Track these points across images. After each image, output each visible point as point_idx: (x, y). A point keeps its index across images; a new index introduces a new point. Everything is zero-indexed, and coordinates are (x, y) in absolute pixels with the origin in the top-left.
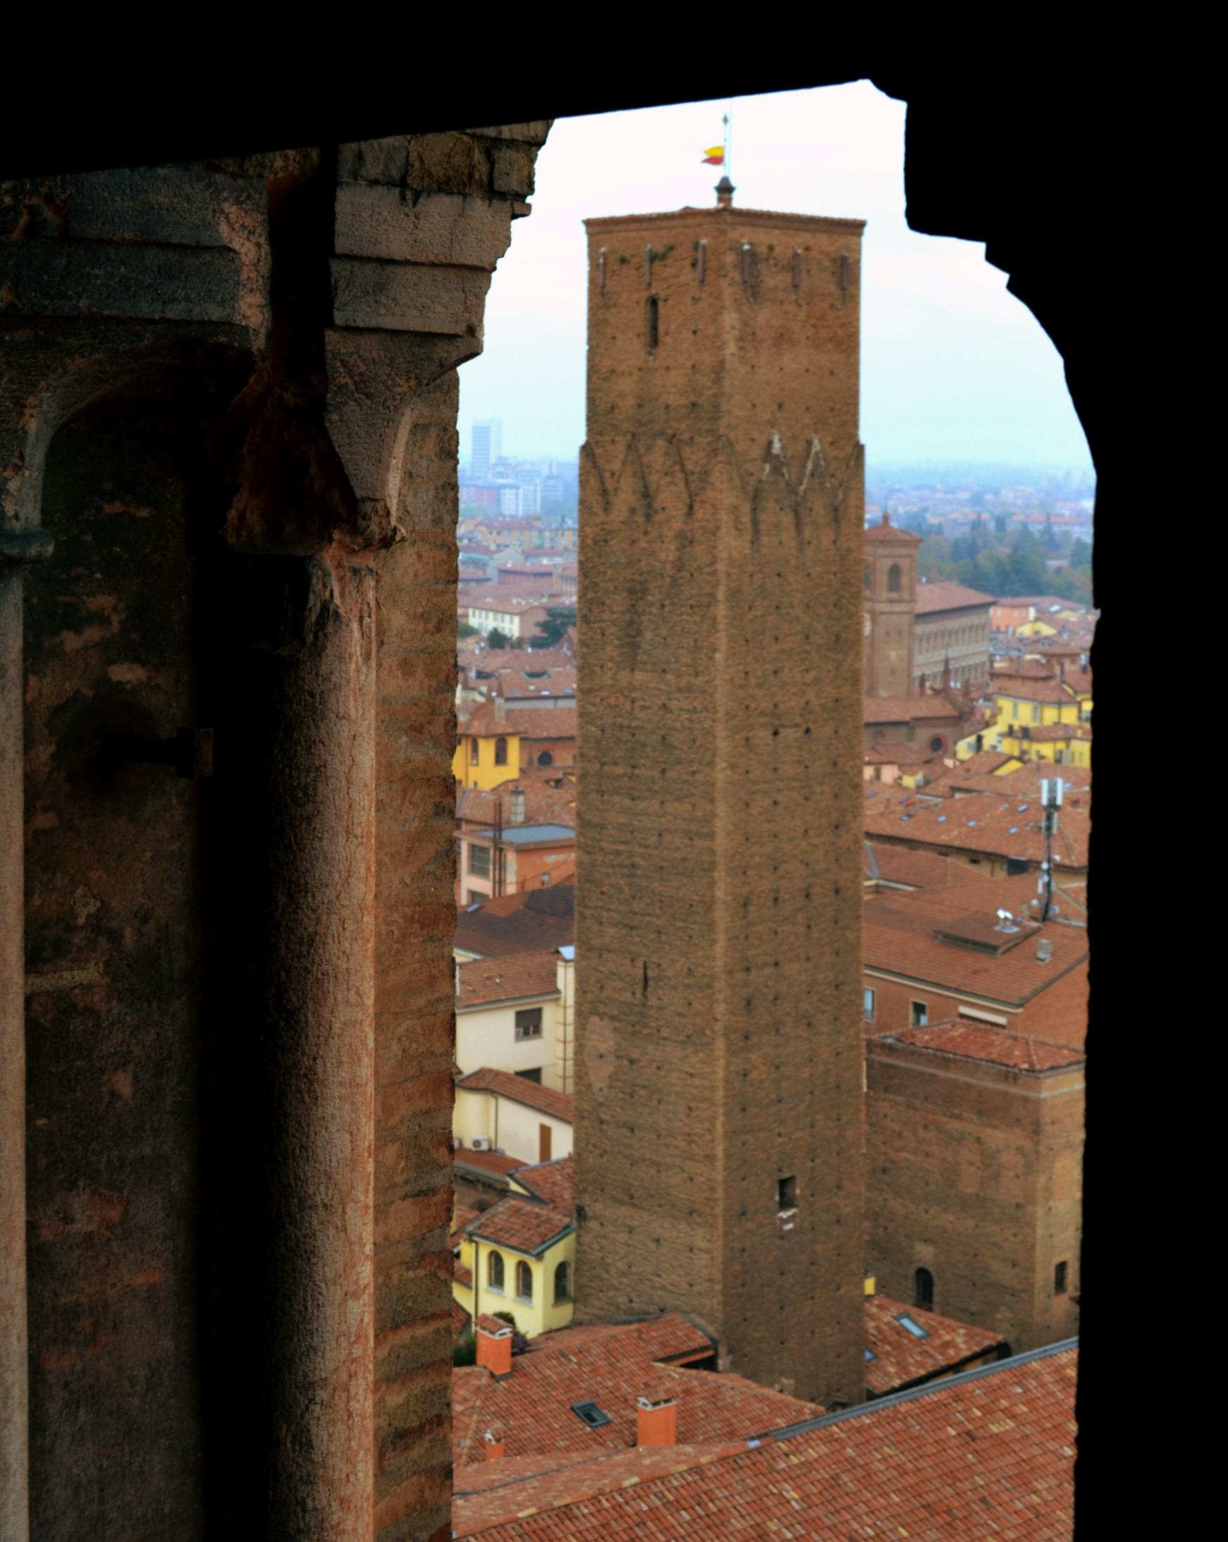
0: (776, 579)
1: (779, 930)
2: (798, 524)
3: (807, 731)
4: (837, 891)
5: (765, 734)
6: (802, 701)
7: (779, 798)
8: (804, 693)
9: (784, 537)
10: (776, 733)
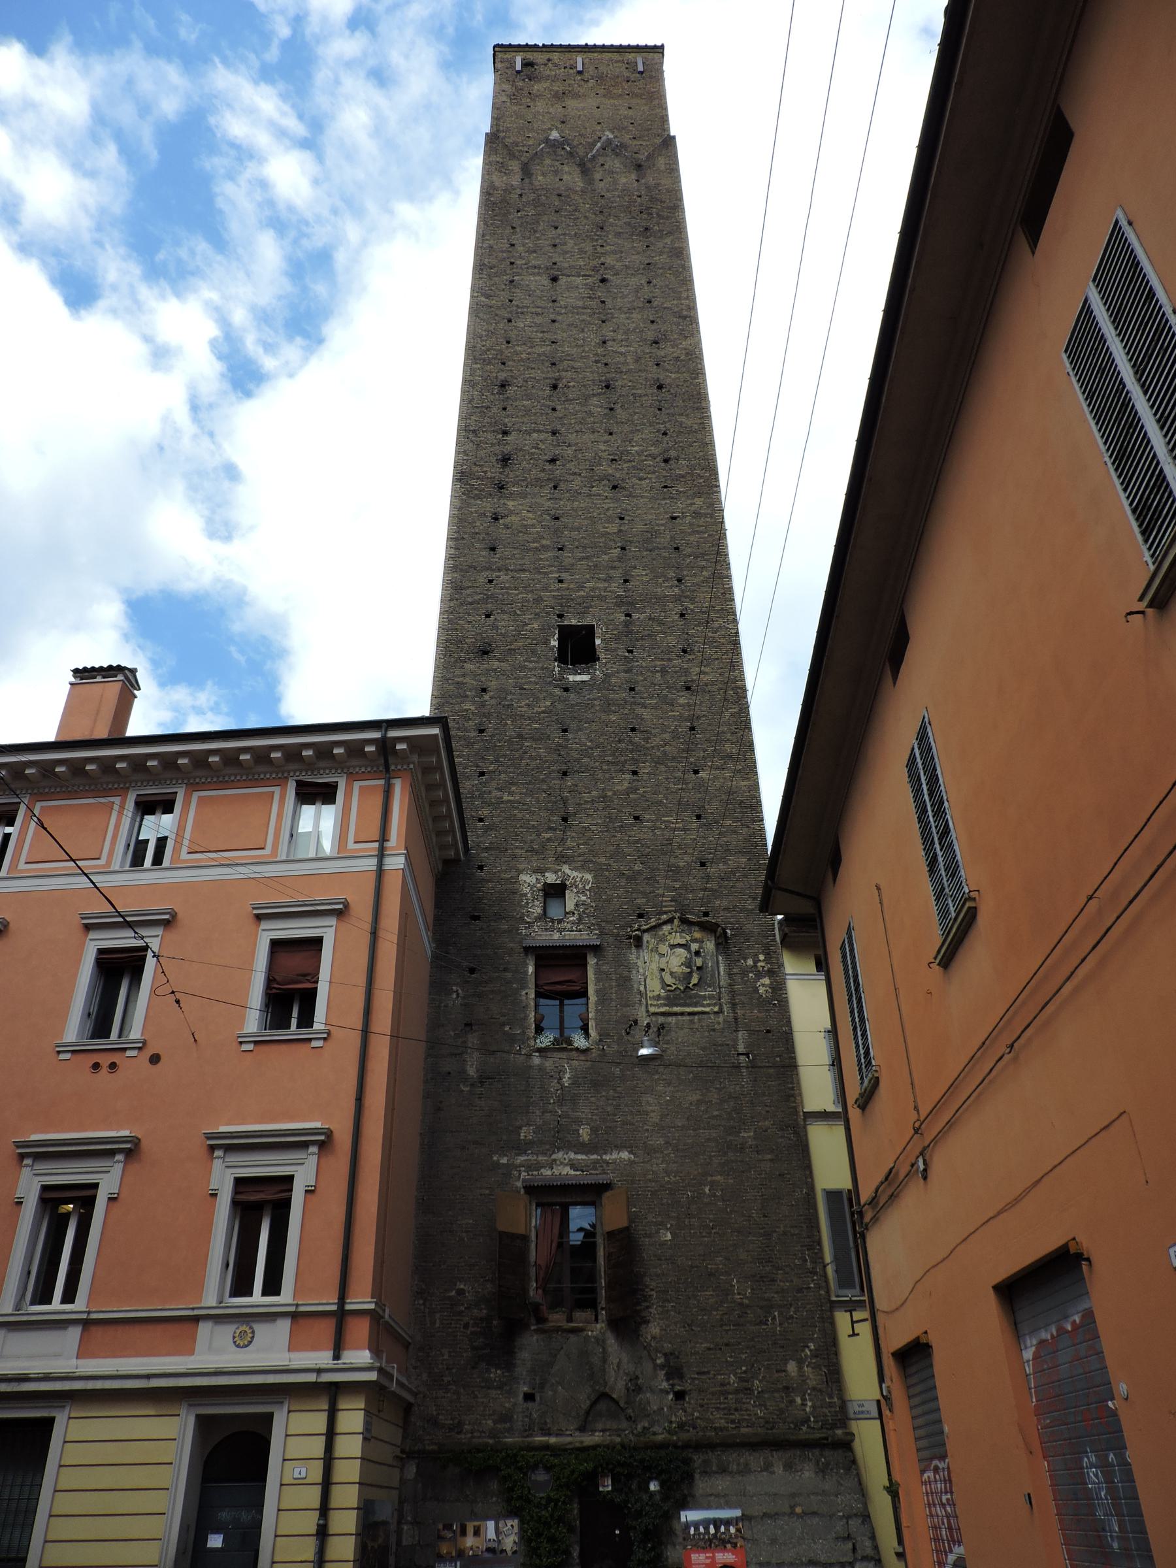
0: (557, 198)
1: (558, 408)
3: (603, 281)
4: (660, 387)
5: (545, 281)
6: (595, 262)
7: (559, 318)
9: (565, 177)
10: (554, 279)
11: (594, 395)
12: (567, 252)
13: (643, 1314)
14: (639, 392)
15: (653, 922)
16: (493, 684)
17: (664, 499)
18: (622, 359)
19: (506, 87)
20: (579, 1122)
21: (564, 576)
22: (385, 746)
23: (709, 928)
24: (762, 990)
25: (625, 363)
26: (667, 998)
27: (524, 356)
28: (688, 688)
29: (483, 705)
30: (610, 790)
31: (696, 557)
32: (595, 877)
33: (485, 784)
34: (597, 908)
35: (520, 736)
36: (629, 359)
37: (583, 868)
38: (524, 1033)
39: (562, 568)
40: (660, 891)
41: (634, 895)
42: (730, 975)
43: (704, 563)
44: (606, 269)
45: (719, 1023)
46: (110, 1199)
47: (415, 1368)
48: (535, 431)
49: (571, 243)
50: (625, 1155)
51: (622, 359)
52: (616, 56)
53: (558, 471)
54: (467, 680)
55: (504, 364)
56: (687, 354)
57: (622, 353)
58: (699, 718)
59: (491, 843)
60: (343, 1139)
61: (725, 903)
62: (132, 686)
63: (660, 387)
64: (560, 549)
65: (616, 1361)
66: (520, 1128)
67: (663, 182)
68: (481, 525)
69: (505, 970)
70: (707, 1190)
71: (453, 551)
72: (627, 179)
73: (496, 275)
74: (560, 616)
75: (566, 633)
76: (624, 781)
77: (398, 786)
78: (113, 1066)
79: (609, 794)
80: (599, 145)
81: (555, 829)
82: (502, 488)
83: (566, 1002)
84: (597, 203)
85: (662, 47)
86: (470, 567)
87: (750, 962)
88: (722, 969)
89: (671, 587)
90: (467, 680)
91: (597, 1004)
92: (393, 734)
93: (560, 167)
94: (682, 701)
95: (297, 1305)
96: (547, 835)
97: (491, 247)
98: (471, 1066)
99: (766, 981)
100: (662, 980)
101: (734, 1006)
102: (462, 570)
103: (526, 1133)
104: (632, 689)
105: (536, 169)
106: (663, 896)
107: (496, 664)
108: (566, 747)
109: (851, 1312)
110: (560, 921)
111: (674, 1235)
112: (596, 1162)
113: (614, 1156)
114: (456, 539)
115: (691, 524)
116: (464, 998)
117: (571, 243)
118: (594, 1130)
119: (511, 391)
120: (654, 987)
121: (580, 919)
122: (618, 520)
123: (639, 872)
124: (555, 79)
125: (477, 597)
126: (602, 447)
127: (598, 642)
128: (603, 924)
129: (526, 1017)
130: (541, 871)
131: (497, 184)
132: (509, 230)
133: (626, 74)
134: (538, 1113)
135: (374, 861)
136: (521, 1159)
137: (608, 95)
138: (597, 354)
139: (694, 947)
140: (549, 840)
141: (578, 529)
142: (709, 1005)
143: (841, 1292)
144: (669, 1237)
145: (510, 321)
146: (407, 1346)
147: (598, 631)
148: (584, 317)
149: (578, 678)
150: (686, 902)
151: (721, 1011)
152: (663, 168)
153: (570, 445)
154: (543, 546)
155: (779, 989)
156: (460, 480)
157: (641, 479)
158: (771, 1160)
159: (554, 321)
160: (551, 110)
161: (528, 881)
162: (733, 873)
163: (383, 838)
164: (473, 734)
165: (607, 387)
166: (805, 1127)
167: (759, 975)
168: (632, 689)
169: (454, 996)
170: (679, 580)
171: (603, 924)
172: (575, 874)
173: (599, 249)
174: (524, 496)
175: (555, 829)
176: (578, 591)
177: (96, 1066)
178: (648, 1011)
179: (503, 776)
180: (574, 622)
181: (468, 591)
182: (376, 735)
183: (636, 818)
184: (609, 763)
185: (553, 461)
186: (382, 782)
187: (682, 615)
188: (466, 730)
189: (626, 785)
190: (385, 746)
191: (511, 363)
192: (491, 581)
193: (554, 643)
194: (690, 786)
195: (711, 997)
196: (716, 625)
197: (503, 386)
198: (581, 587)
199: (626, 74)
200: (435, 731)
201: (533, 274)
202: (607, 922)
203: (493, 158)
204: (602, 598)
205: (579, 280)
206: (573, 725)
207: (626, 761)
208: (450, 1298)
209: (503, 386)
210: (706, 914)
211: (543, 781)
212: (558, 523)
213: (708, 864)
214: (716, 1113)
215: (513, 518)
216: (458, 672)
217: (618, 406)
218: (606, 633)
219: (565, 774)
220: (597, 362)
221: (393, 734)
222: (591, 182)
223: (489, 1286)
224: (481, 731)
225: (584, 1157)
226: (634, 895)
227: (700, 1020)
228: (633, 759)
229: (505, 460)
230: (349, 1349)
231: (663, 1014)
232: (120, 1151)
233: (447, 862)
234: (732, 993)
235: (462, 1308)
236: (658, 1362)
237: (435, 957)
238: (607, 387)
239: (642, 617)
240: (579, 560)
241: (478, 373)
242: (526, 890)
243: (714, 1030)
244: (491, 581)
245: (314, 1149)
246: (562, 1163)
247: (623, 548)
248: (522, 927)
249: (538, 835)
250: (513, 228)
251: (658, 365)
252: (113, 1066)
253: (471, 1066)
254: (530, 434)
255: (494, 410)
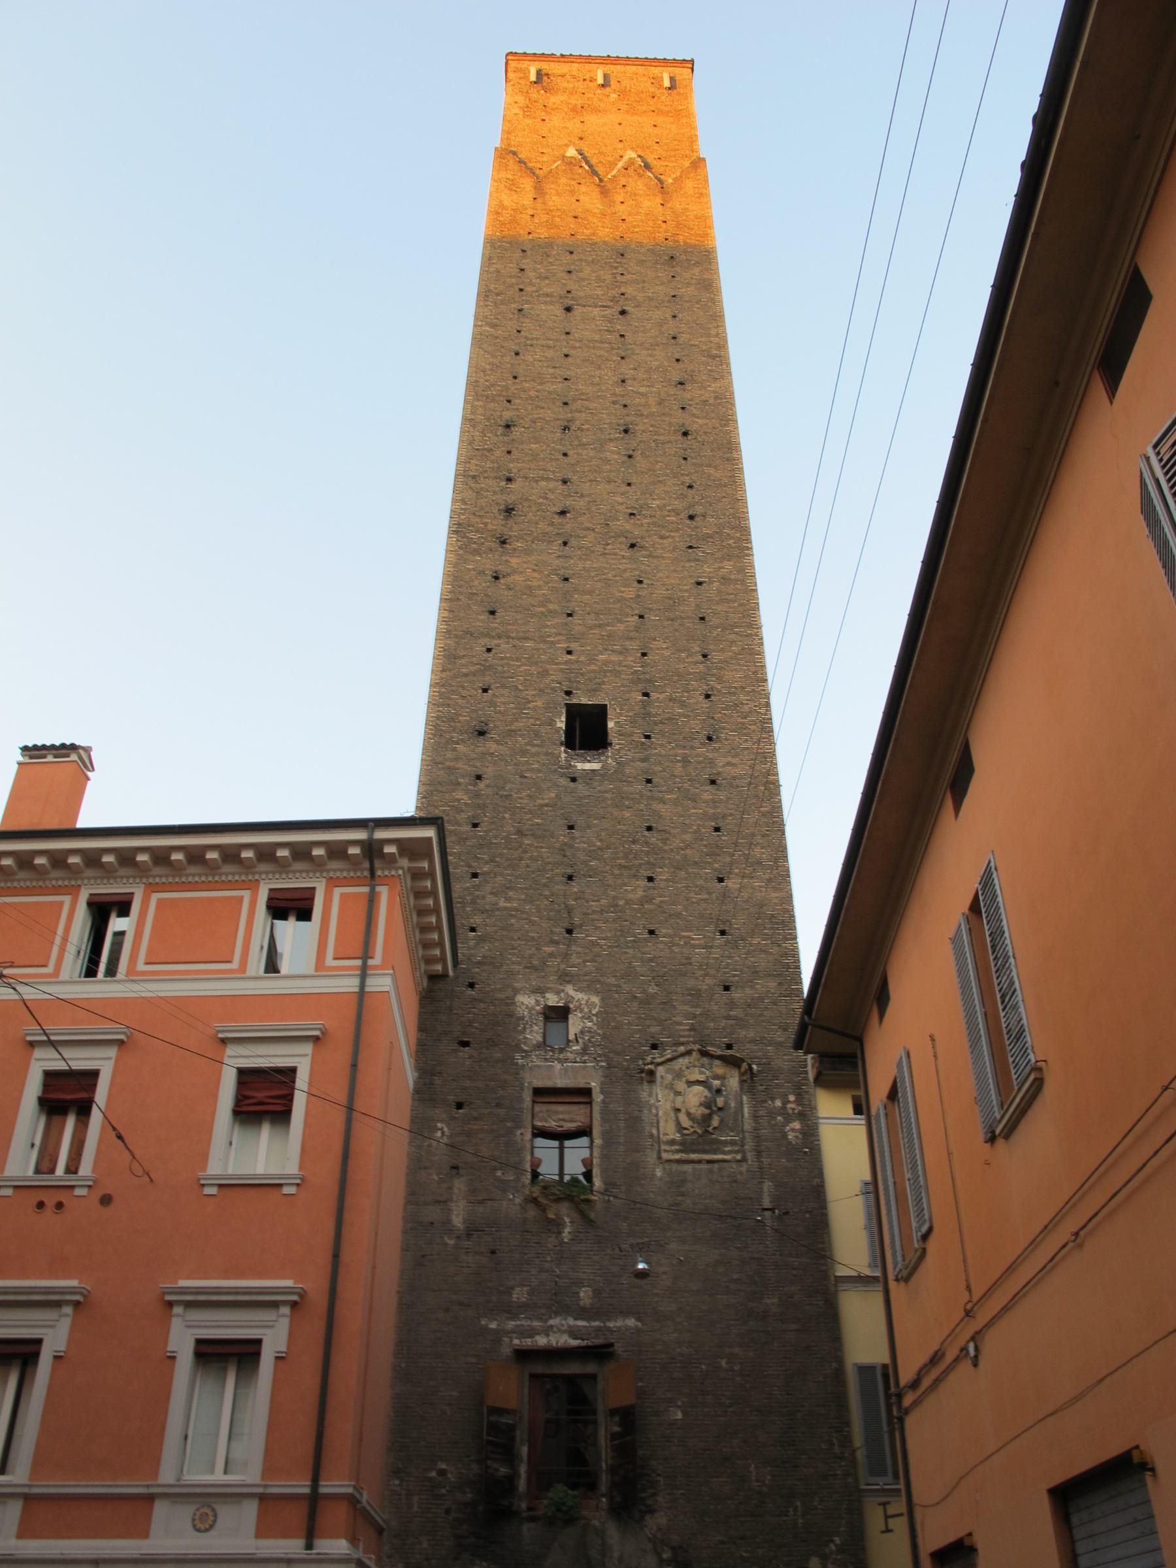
1: (570, 453)
2: (604, 191)
3: (623, 313)
4: (685, 434)
5: (559, 311)
6: (615, 292)
7: (572, 352)
8: (619, 287)
9: (582, 198)
10: (568, 309)
11: (611, 440)
12: (583, 279)
13: (649, 1502)
14: (662, 438)
15: (669, 1054)
16: (489, 771)
17: (689, 561)
18: (643, 400)
19: (520, 98)
20: (579, 1283)
21: (573, 646)
22: (372, 850)
23: (733, 1062)
24: (791, 1136)
25: (646, 405)
26: (682, 1143)
27: (532, 393)
28: (713, 782)
29: (477, 795)
30: (621, 899)
31: (724, 629)
32: (602, 1000)
33: (477, 887)
34: (604, 1037)
35: (520, 832)
36: (651, 401)
37: (589, 988)
38: (518, 1179)
39: (572, 638)
40: (678, 1019)
41: (648, 1022)
42: (755, 1117)
43: (733, 636)
44: (627, 299)
45: (741, 1173)
46: (56, 1357)
47: (389, 1557)
48: (543, 479)
49: (587, 270)
50: (631, 1322)
51: (643, 400)
52: (640, 69)
53: (568, 524)
54: (460, 765)
55: (509, 401)
56: (716, 398)
57: (642, 394)
58: (724, 817)
59: (484, 957)
60: (318, 1297)
61: (751, 1034)
62: (86, 766)
63: (685, 434)
64: (570, 615)
65: (616, 1555)
66: (512, 1288)
67: (690, 207)
68: (481, 584)
69: (498, 1105)
70: (723, 1362)
71: (446, 614)
72: (651, 203)
73: (503, 302)
74: (568, 693)
75: (574, 712)
76: (637, 889)
77: (383, 892)
78: (60, 1205)
79: (621, 903)
80: (620, 164)
81: (557, 943)
82: (504, 542)
83: (567, 1143)
84: (617, 227)
85: (692, 61)
86: (467, 632)
87: (778, 1103)
88: (746, 1110)
89: (696, 663)
90: (460, 765)
91: (602, 1147)
92: (380, 834)
93: (577, 187)
94: (706, 796)
95: (265, 1486)
96: (549, 949)
97: (498, 271)
98: (458, 1215)
99: (797, 1125)
100: (678, 1123)
101: (759, 1153)
102: (456, 636)
103: (519, 1295)
104: (649, 781)
105: (549, 188)
106: (681, 1024)
107: (493, 747)
108: (572, 847)
109: (884, 1504)
110: (562, 1050)
111: (685, 1413)
112: (598, 1329)
113: (619, 1323)
114: (450, 600)
115: (719, 592)
116: (451, 1136)
117: (587, 270)
118: (597, 1293)
119: (516, 432)
120: (669, 1130)
121: (585, 1051)
122: (636, 584)
123: (654, 996)
124: (573, 92)
125: (473, 668)
126: (619, 499)
127: (610, 724)
128: (611, 1055)
129: (521, 1162)
130: (540, 991)
131: (507, 203)
132: (518, 254)
133: (652, 89)
134: (534, 1272)
135: (355, 982)
136: (511, 1324)
137: (632, 111)
138: (615, 395)
139: (716, 1083)
140: (551, 955)
141: (591, 592)
142: (730, 1152)
143: (873, 1480)
144: (680, 1416)
145: (517, 354)
146: (380, 1531)
147: (610, 713)
148: (602, 353)
149: (587, 766)
150: (707, 1032)
151: (744, 1160)
152: (691, 192)
153: (582, 496)
154: (550, 611)
155: (810, 1135)
156: (456, 532)
157: (662, 537)
158: (797, 1330)
159: (566, 356)
160: (568, 125)
161: (526, 1002)
162: (761, 999)
163: (366, 955)
164: (467, 828)
165: (626, 431)
166: (836, 1293)
167: (788, 1119)
168: (649, 781)
169: (439, 1134)
170: (705, 656)
171: (611, 1055)
172: (580, 996)
173: (619, 278)
174: (527, 552)
175: (557, 943)
176: (589, 665)
177: (41, 1205)
178: (660, 1158)
179: (499, 878)
180: (584, 701)
181: (463, 661)
182: (360, 835)
183: (651, 932)
184: (621, 867)
185: (563, 513)
186: (366, 889)
187: (708, 696)
188: (458, 824)
189: (640, 893)
190: (372, 850)
191: (518, 401)
192: (489, 650)
193: (561, 724)
194: (714, 896)
195: (733, 1143)
196: (746, 708)
197: (508, 426)
198: (592, 660)
199: (652, 89)
200: (430, 833)
201: (545, 303)
202: (616, 1053)
203: (503, 175)
204: (617, 674)
205: (596, 311)
206: (580, 821)
207: (640, 865)
208: (430, 1479)
209: (508, 426)
210: (729, 1047)
211: (545, 885)
212: (567, 584)
213: (733, 988)
214: (736, 1276)
215: (517, 578)
216: (449, 755)
217: (637, 454)
218: (621, 715)
219: (570, 878)
220: (614, 403)
221: (380, 834)
222: (611, 204)
223: (474, 1466)
224: (475, 825)
225: (584, 1323)
226: (648, 1022)
227: (720, 1169)
228: (648, 863)
229: (509, 511)
230: (323, 1537)
231: (678, 1161)
232: (67, 1303)
233: (433, 978)
234: (758, 1138)
235: (444, 1491)
236: (665, 1556)
237: (417, 1091)
238: (626, 431)
239: (662, 697)
240: (591, 628)
241: (481, 411)
242: (521, 1011)
243: (735, 1181)
244: (489, 650)
245: (286, 1310)
246: (560, 1331)
247: (641, 617)
248: (517, 1056)
249: (539, 949)
250: (524, 251)
251: (683, 408)
252: (60, 1205)
253: (458, 1215)
254: (537, 481)
255: (498, 453)
